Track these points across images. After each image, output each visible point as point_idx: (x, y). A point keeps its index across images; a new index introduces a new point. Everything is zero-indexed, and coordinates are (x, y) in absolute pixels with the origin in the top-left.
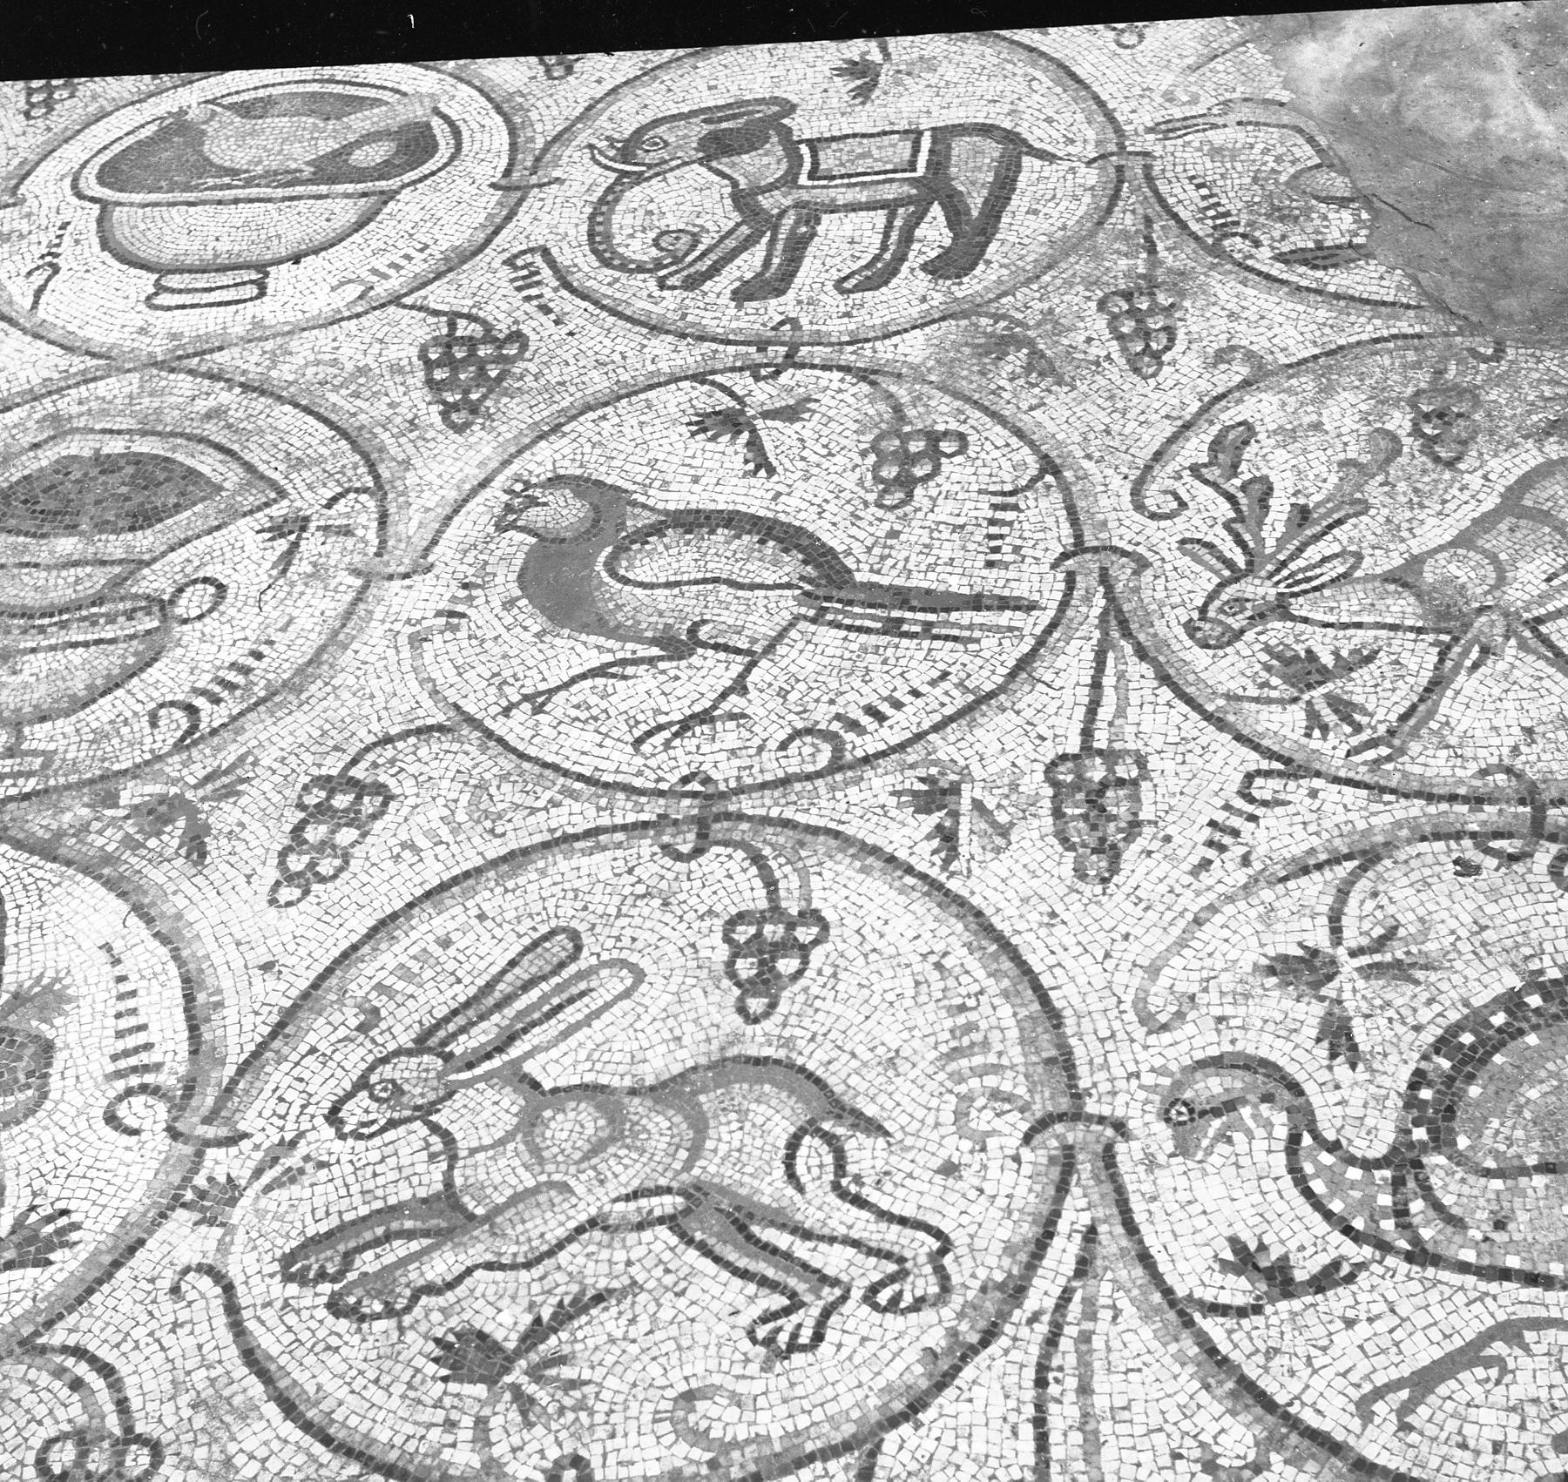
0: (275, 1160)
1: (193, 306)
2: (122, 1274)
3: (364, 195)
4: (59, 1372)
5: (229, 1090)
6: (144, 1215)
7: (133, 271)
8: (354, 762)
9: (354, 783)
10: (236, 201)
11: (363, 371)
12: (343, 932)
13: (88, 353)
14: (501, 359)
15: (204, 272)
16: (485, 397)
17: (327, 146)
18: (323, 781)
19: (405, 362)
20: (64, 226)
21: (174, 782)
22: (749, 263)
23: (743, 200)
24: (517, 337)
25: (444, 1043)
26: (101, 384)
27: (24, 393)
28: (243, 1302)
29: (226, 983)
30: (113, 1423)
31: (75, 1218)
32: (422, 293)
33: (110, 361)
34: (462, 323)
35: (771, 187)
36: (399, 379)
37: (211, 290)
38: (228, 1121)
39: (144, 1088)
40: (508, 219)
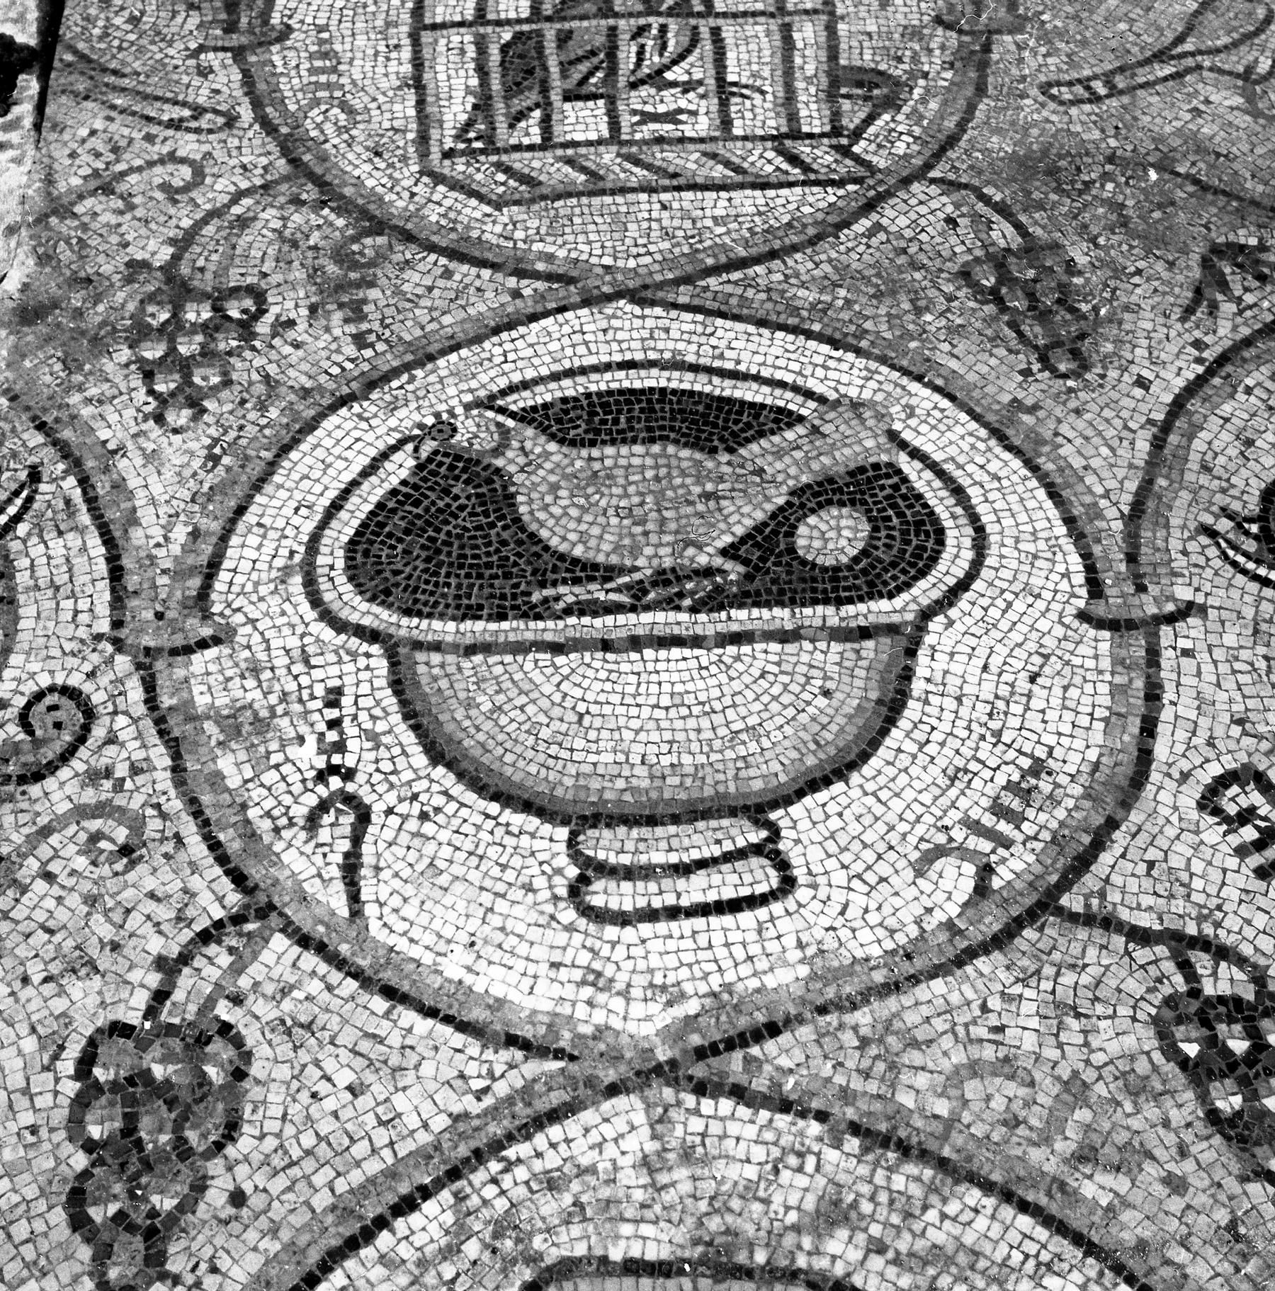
1: (673, 913)
3: (865, 633)
7: (517, 819)
10: (635, 643)
13: (512, 1041)
15: (652, 821)
17: (743, 517)
19: (1142, 1066)
20: (334, 698)
26: (572, 1126)
27: (424, 1155)
32: (1090, 881)
33: (576, 1072)
34: (1202, 962)
36: (1151, 1112)
37: (683, 870)
40: (1153, 694)
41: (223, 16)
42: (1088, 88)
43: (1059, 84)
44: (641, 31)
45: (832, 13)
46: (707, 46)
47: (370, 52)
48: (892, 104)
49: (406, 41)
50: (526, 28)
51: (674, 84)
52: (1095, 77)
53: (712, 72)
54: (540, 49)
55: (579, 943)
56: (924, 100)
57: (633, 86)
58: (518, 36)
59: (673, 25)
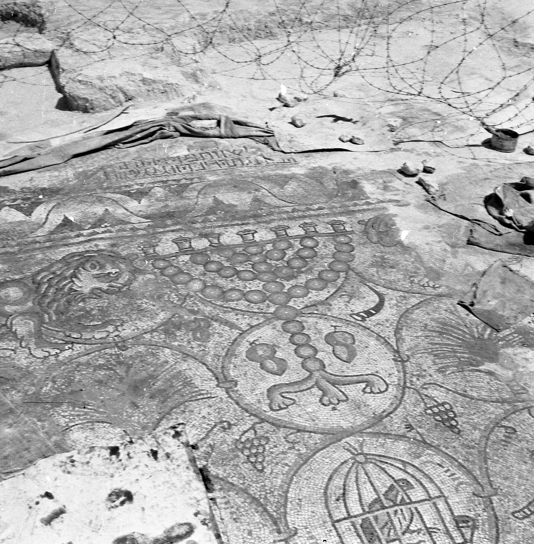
41: (275, 527)
42: (524, 512)
43: (516, 512)
44: (396, 512)
45: (444, 496)
46: (416, 514)
47: (324, 534)
48: (474, 528)
49: (332, 528)
50: (364, 517)
51: (414, 531)
52: (524, 508)
53: (422, 525)
54: (371, 524)
56: (483, 525)
57: (403, 534)
58: (363, 520)
59: (402, 507)
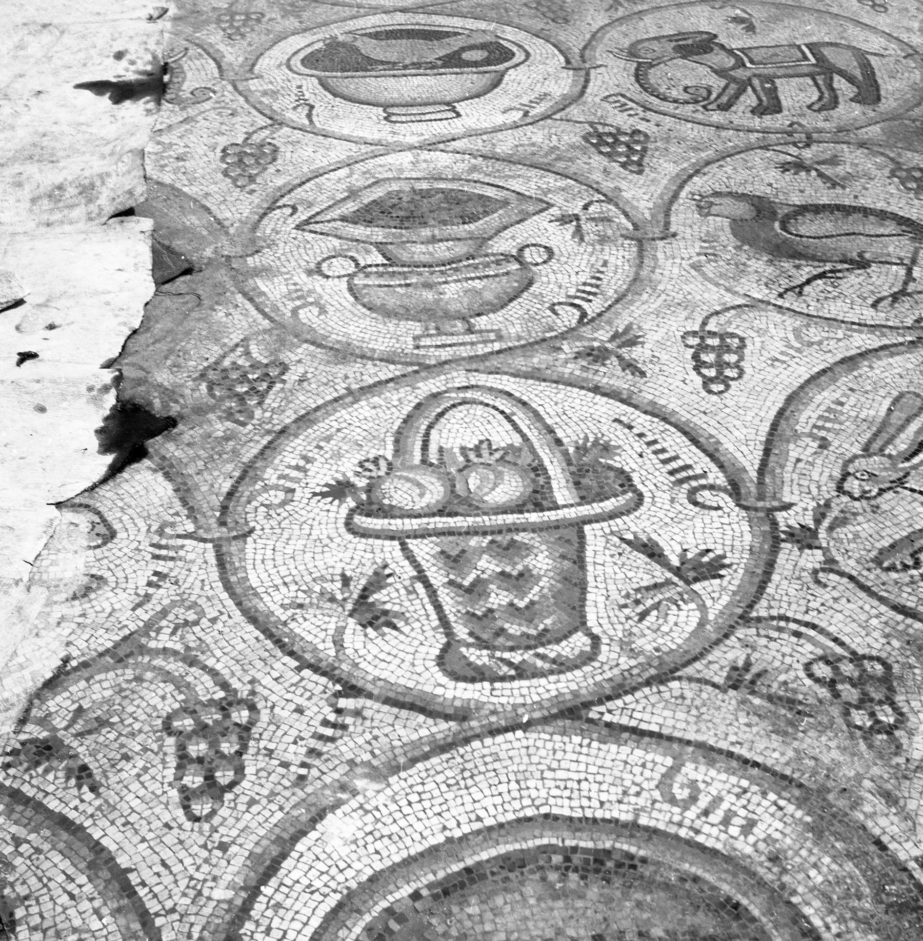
0: (824, 516)
2: (775, 577)
4: (780, 629)
5: (761, 483)
6: (761, 548)
8: (704, 324)
9: (713, 334)
11: (555, 148)
12: (768, 403)
14: (638, 142)
16: (641, 159)
18: (694, 334)
21: (595, 339)
22: (749, 99)
23: (720, 72)
24: (636, 132)
25: (881, 450)
28: (869, 584)
29: (714, 432)
30: (839, 650)
31: (719, 552)
35: (733, 68)
38: (774, 497)
39: (704, 487)
40: (587, 81)
55: (388, 127)
